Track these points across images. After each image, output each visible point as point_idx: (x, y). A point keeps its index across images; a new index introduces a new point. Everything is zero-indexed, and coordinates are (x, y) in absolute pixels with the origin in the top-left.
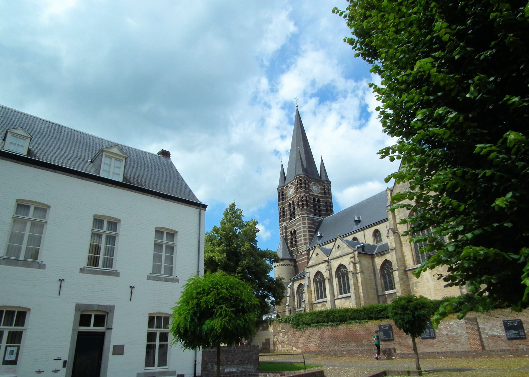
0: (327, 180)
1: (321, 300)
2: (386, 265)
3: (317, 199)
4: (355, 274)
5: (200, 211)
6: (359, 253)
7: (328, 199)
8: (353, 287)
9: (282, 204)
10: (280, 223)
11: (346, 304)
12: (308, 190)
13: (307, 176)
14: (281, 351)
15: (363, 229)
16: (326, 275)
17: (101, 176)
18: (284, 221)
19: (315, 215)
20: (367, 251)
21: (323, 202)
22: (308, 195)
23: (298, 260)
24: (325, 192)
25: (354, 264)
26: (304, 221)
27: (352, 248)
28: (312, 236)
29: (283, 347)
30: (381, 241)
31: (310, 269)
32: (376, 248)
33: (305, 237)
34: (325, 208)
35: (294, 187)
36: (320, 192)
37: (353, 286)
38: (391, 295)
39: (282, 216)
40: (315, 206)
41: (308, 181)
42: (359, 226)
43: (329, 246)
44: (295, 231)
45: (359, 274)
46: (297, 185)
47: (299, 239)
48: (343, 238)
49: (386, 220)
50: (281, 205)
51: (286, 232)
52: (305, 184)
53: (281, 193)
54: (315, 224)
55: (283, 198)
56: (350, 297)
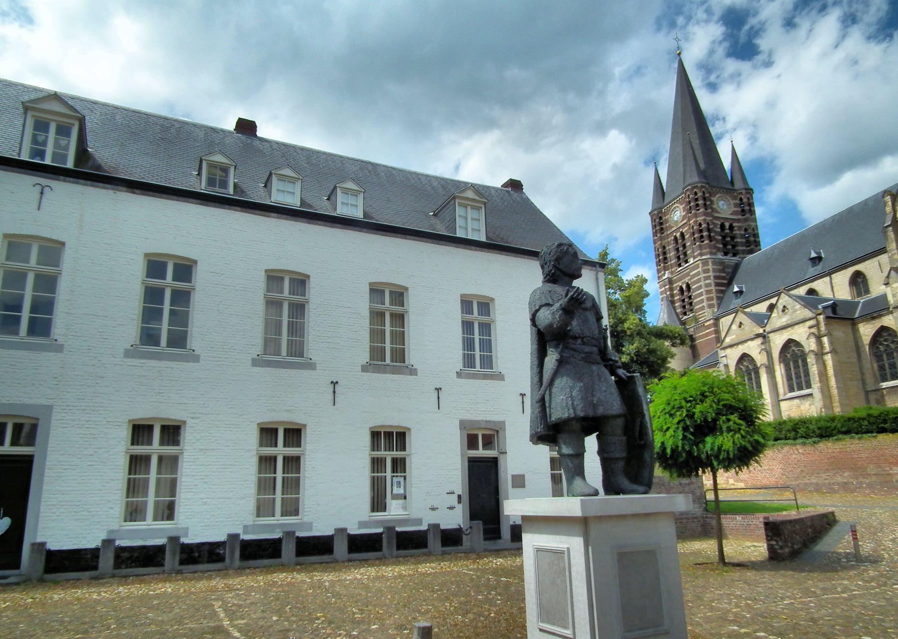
0: (747, 187)
2: (881, 336)
3: (727, 225)
4: (820, 354)
5: (597, 274)
6: (827, 318)
7: (748, 223)
8: (817, 379)
9: (661, 239)
10: (658, 273)
11: (802, 408)
12: (709, 211)
13: (708, 184)
15: (829, 274)
16: (760, 359)
17: (458, 235)
18: (665, 269)
19: (726, 254)
20: (841, 312)
21: (740, 228)
22: (711, 218)
23: (697, 335)
24: (743, 211)
25: (819, 338)
26: (705, 268)
27: (812, 309)
28: (723, 292)
30: (867, 291)
31: (728, 351)
32: (858, 305)
33: (709, 296)
34: (744, 240)
35: (681, 207)
36: (734, 211)
37: (817, 376)
38: (893, 389)
39: (662, 261)
40: (724, 237)
41: (709, 193)
42: (819, 268)
43: (762, 308)
44: (688, 286)
45: (829, 354)
46: (690, 202)
47: (698, 299)
48: (789, 290)
49: (882, 251)
50: (659, 242)
51: (671, 289)
52: (705, 199)
53: (657, 220)
54: (727, 270)
55: (662, 229)
56: (811, 395)
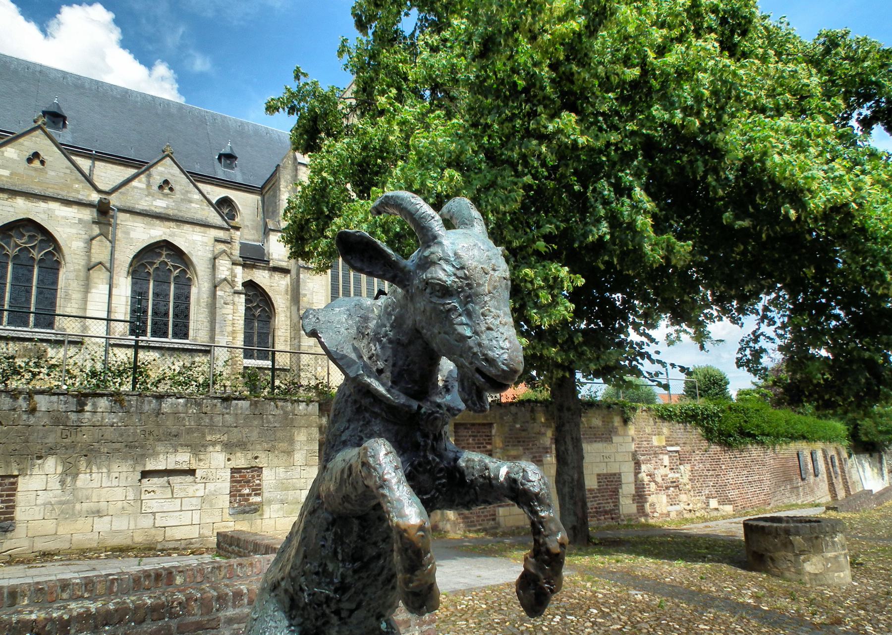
1: (170, 341)
14: (668, 515)
29: (673, 502)
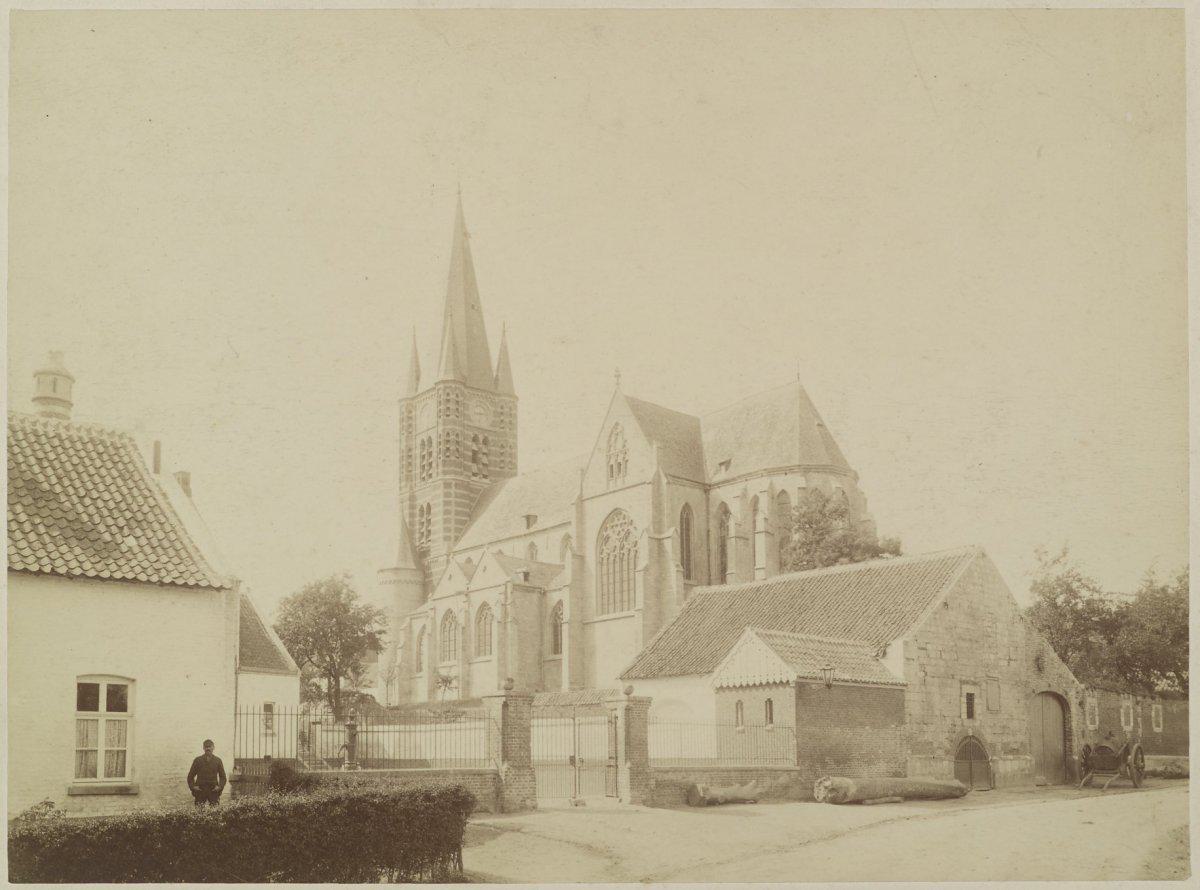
3: (481, 438)
